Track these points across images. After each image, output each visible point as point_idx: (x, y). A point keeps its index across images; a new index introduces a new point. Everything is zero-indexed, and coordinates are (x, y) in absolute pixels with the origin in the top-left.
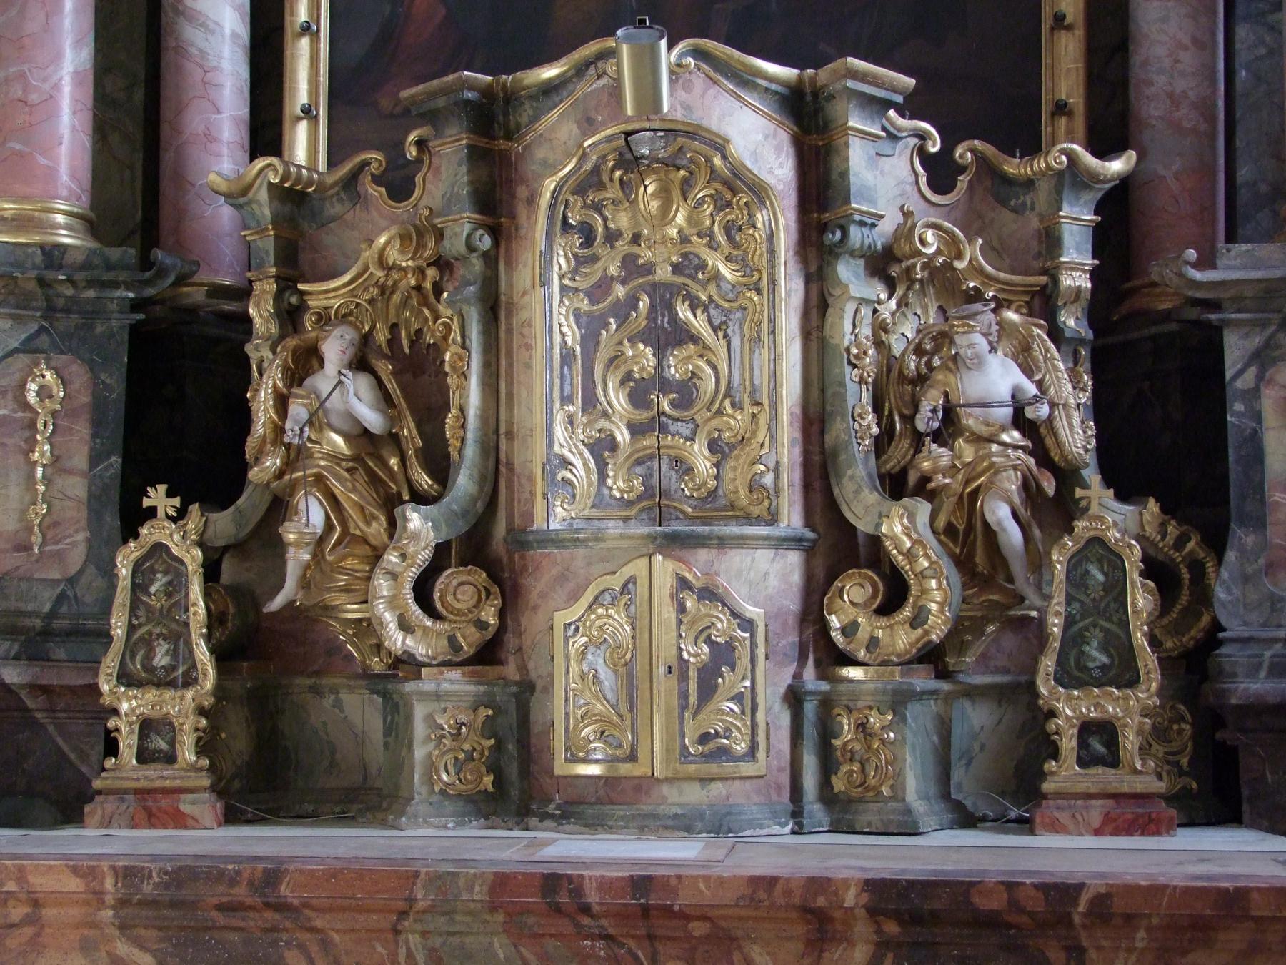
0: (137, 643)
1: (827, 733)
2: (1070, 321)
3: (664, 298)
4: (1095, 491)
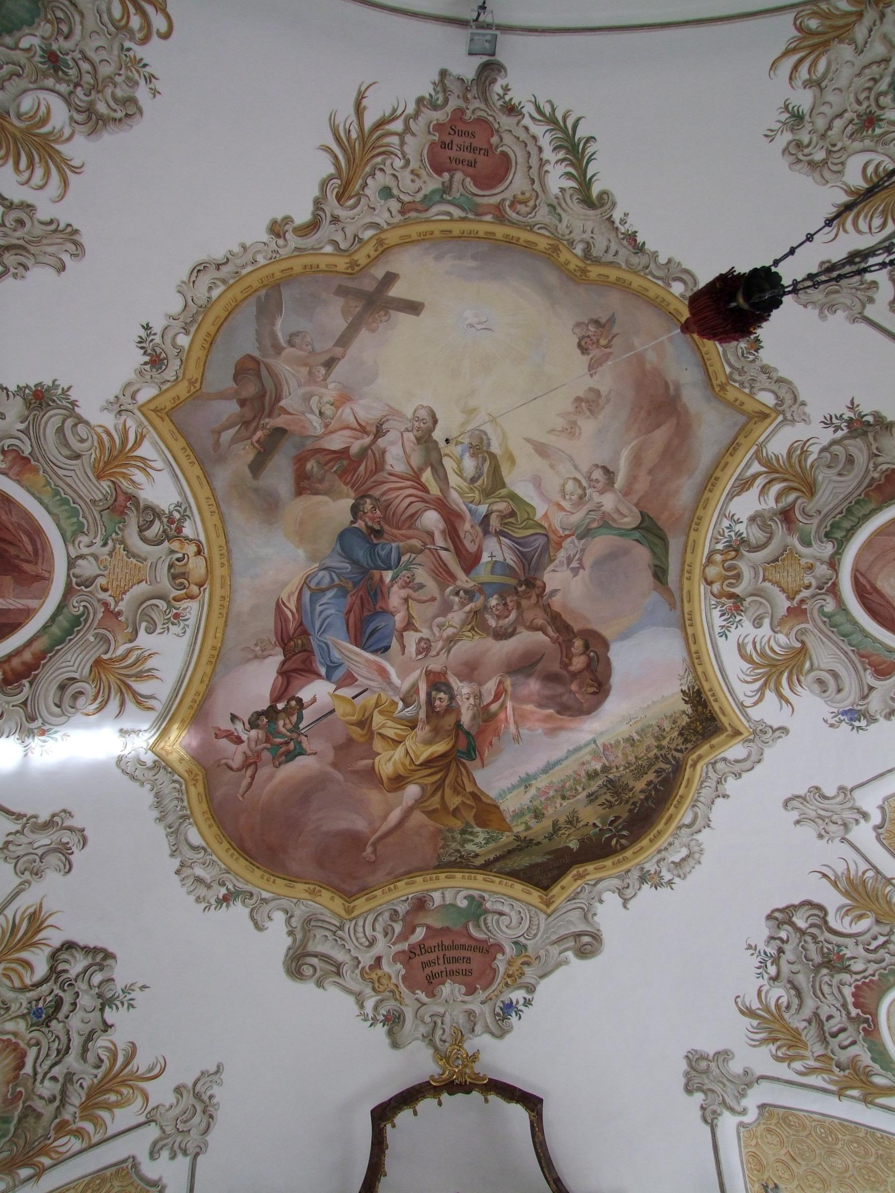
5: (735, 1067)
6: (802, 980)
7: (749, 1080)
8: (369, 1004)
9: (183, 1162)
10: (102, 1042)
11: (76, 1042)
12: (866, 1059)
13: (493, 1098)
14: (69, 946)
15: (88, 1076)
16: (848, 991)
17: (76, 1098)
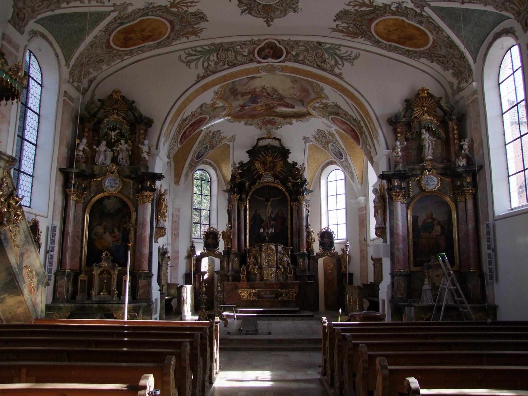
0: (242, 273)
3: (269, 255)
4: (290, 264)
7: (311, 141)
8: (257, 127)
9: (232, 143)
10: (220, 137)
12: (326, 146)
13: (274, 140)
14: (214, 132)
15: (219, 140)
16: (326, 141)
17: (218, 142)
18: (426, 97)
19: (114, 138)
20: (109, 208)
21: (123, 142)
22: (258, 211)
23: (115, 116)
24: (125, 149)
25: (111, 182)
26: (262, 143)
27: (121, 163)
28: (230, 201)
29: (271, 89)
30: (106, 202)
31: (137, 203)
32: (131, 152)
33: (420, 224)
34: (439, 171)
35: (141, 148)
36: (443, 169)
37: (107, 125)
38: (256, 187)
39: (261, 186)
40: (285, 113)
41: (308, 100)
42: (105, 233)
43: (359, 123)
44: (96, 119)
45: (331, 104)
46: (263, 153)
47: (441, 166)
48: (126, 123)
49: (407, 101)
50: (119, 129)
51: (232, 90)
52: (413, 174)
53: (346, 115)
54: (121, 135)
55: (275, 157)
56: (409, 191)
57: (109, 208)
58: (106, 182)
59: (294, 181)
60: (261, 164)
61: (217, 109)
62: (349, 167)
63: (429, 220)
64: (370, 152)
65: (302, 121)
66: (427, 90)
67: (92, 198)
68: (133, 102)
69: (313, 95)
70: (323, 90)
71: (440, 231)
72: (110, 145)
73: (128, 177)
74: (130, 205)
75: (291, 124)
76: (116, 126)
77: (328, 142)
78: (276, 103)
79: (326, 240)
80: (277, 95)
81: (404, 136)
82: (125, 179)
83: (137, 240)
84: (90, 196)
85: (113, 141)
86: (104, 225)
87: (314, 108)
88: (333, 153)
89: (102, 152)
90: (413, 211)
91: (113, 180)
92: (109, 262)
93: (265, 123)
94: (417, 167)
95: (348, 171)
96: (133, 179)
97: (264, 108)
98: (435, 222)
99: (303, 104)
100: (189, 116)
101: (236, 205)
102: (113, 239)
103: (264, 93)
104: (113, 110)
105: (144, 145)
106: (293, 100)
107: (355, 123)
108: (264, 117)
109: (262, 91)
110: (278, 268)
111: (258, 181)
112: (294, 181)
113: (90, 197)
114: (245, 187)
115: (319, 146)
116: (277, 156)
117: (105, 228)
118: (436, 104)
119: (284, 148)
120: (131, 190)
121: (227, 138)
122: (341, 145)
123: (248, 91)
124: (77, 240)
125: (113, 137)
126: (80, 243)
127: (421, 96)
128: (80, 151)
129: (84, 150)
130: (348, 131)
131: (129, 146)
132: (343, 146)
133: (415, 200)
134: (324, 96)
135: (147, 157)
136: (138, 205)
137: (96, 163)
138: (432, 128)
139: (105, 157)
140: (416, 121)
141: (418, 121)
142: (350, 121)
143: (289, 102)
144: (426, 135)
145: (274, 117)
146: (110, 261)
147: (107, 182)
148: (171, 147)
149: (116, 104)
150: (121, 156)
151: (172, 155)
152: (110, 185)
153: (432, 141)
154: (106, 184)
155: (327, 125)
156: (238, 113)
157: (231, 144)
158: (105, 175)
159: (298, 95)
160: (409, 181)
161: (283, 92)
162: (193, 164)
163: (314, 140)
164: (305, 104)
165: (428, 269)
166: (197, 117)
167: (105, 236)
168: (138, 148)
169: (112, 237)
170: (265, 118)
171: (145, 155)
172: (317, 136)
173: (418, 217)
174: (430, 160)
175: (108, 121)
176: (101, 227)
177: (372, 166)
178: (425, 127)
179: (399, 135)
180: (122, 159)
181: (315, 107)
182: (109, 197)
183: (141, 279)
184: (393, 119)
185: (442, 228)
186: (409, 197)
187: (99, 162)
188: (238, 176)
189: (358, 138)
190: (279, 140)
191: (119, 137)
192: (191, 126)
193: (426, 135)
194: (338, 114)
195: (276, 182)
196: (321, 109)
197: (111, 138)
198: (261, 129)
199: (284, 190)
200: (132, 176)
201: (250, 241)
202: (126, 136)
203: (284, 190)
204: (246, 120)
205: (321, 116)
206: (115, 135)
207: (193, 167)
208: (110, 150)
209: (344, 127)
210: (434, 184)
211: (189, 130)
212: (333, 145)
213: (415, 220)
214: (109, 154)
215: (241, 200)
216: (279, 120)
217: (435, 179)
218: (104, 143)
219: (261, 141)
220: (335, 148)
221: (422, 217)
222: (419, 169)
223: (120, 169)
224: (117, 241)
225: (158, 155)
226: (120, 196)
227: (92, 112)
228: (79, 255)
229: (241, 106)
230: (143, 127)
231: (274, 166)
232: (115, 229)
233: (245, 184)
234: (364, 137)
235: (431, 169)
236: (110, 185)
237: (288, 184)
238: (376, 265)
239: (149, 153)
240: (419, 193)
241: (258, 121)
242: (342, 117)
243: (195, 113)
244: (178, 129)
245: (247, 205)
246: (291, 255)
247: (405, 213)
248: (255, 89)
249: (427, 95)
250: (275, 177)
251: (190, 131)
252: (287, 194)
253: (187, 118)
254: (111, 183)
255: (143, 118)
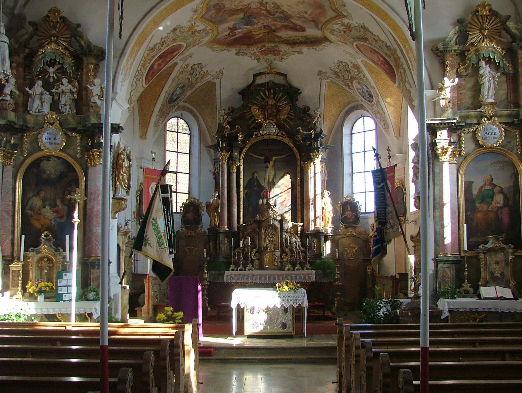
1: (282, 264)
2: (298, 235)
5: (327, 75)
6: (342, 71)
7: (329, 77)
8: (253, 58)
9: (218, 80)
11: (197, 74)
13: (277, 76)
16: (350, 76)
17: (199, 79)
18: (487, 16)
19: (53, 77)
20: (48, 172)
21: (65, 81)
22: (256, 175)
23: (53, 46)
24: (69, 91)
25: (51, 136)
26: (260, 81)
27: (63, 110)
28: (216, 161)
29: (272, 5)
30: (45, 165)
31: (87, 165)
32: (77, 95)
33: (475, 192)
34: (504, 120)
35: (91, 90)
36: (509, 116)
37: (42, 58)
38: (253, 140)
39: (260, 139)
40: (293, 38)
41: (324, 20)
42: (44, 207)
43: (395, 52)
44: (27, 51)
45: (357, 25)
46: (262, 94)
47: (506, 112)
48: (69, 55)
49: (460, 22)
50: (59, 63)
51: (218, 7)
52: (466, 124)
53: (376, 41)
54: (62, 71)
55: (279, 101)
56: (460, 147)
57: (48, 172)
58: (44, 137)
59: (305, 132)
60: (259, 110)
61: (197, 34)
62: (381, 112)
63: (488, 187)
64: (410, 93)
65: (316, 50)
66: (489, 5)
67: (25, 159)
68: (79, 25)
69: (331, 14)
70: (344, 5)
71: (502, 202)
72: (48, 86)
73: (73, 130)
74: (78, 168)
75: (300, 53)
76: (55, 60)
77: (352, 79)
78: (279, 24)
79: (348, 214)
80: (280, 13)
81: (455, 70)
82: (69, 133)
83: (88, 216)
84: (23, 156)
85: (52, 80)
86: (42, 196)
87: (332, 31)
88: (360, 94)
89: (37, 96)
90: (465, 175)
91: (53, 134)
92: (51, 246)
93: (265, 53)
94: (472, 113)
95: (380, 119)
96: (80, 132)
97: (263, 31)
98: (497, 189)
99: (317, 26)
100: (157, 44)
101: (225, 166)
102: (55, 214)
103: (262, 10)
104: (51, 36)
105: (95, 85)
106: (303, 19)
107: (388, 52)
108: (264, 44)
109: (259, 8)
110: (283, 251)
111: (256, 133)
112: (305, 132)
113: (22, 158)
114: (238, 141)
115: (341, 84)
116: (281, 98)
117: (44, 200)
118: (502, 25)
119: (291, 86)
120: (78, 148)
121: (212, 74)
122: (370, 83)
123: (239, 8)
124: (6, 216)
125: (52, 75)
126: (11, 220)
127: (481, 14)
128: (6, 95)
129: (12, 94)
130: (379, 63)
131: (74, 87)
132: (373, 84)
133: (469, 159)
134: (346, 15)
135: (99, 102)
136: (87, 168)
137: (29, 111)
138: (494, 59)
139: (42, 103)
140: (472, 50)
141: (474, 49)
142: (381, 48)
143: (299, 23)
144: (485, 70)
145: (277, 44)
146: (51, 244)
147: (44, 138)
148: (134, 88)
149: (55, 27)
150: (63, 101)
151: (135, 99)
152: (49, 141)
153: (494, 78)
154: (44, 139)
155: (351, 55)
156: (227, 38)
157: (217, 81)
158: (41, 128)
159: (309, 12)
160: (461, 133)
161: (289, 9)
162: (165, 110)
163: (333, 76)
164: (320, 25)
165: (484, 253)
166: (168, 45)
167: (44, 210)
168: (86, 89)
169: (54, 211)
170: (264, 46)
171: (96, 99)
172: (337, 70)
173: (473, 182)
174: (492, 104)
175: (43, 53)
176: (38, 198)
177: (413, 112)
178: (484, 59)
179: (448, 69)
180: (65, 105)
181: (334, 30)
182: (48, 158)
183: (94, 268)
184: (440, 47)
185: (506, 198)
186: (460, 155)
187: (33, 110)
188: (227, 126)
189: (393, 72)
190: (285, 75)
191: (59, 75)
192: (160, 57)
193: (485, 70)
194: (366, 40)
195: (280, 134)
196: (343, 33)
197: (49, 76)
198: (258, 60)
199: (291, 145)
200: (79, 128)
201: (244, 216)
202: (70, 73)
203: (291, 145)
204: (238, 48)
205: (342, 42)
206: (54, 73)
207: (165, 116)
208: (48, 93)
209: (375, 57)
210: (495, 138)
211: (157, 63)
212: (359, 83)
213: (468, 186)
214: (47, 98)
215: (231, 159)
216: (283, 48)
217: (497, 130)
218: (40, 83)
219: (259, 77)
220: (361, 86)
221: (478, 184)
222: (476, 117)
223: (63, 118)
224: (61, 217)
225: (115, 99)
226: (63, 155)
227: (22, 40)
228: (10, 237)
229: (229, 28)
230: (94, 61)
231: (278, 112)
232: (58, 202)
233: (238, 136)
234: (402, 71)
235: (491, 117)
236: (49, 141)
237: (297, 137)
238: (417, 247)
239: (100, 97)
240: (474, 150)
241: (255, 49)
242: (371, 44)
243: (166, 40)
244: (142, 62)
245: (240, 165)
246: (301, 234)
247: (455, 177)
248: (249, 4)
249: (489, 12)
250: (280, 126)
251: (159, 65)
252: (295, 150)
253: (155, 46)
254: (50, 139)
255: (93, 48)
